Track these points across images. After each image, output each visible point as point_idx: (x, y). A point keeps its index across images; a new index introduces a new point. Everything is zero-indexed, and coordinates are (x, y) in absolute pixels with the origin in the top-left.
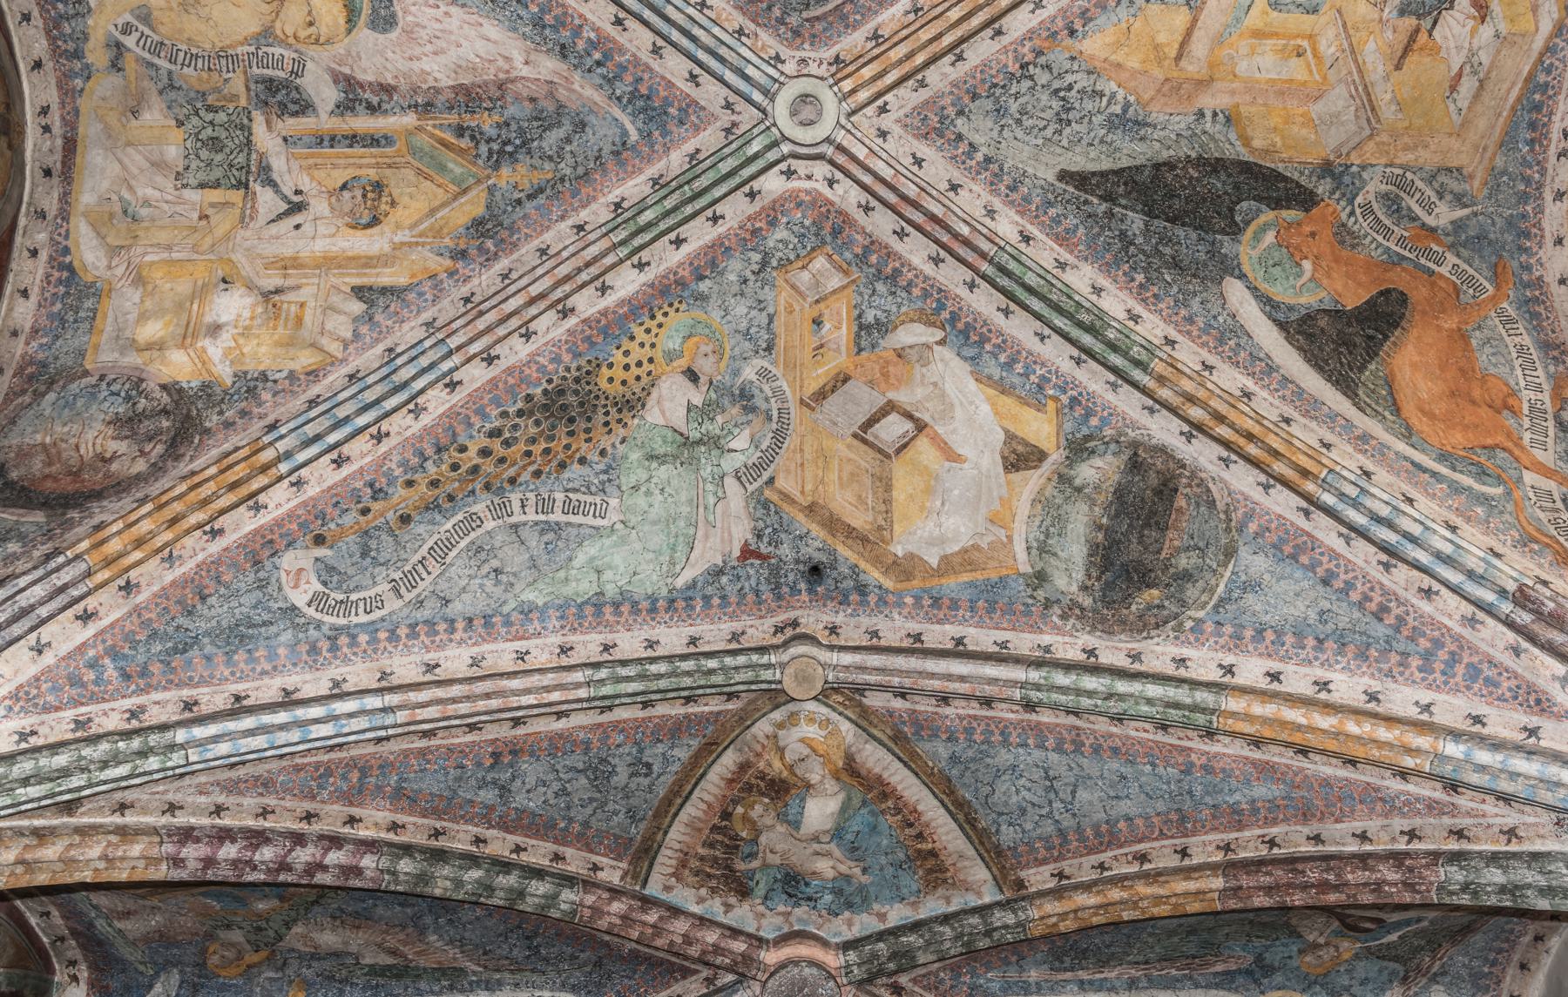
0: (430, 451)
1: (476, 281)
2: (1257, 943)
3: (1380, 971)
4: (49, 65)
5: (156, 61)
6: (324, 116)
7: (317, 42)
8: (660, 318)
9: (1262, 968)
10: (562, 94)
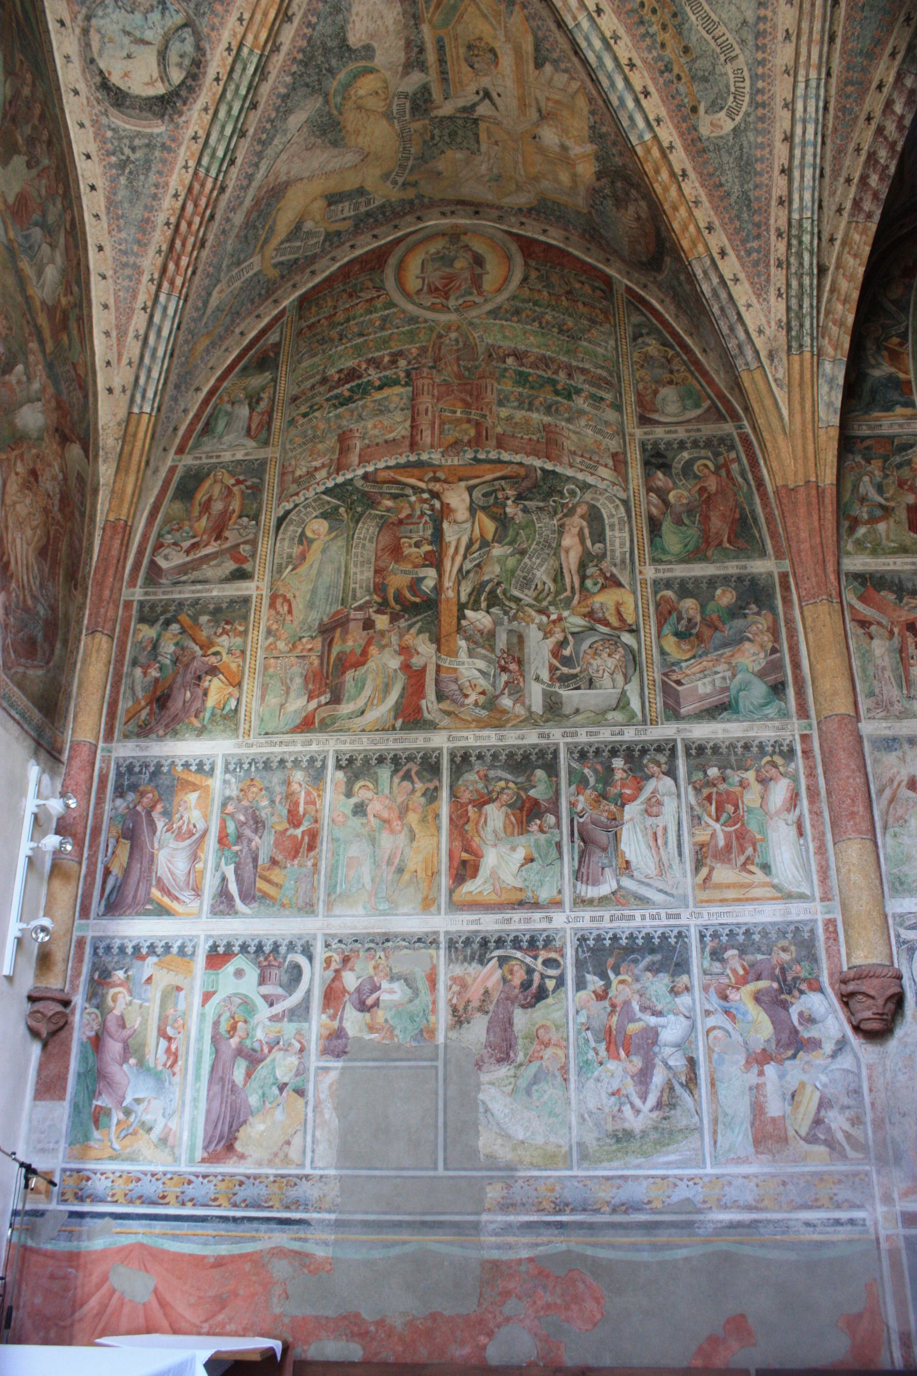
0: (642, 30)
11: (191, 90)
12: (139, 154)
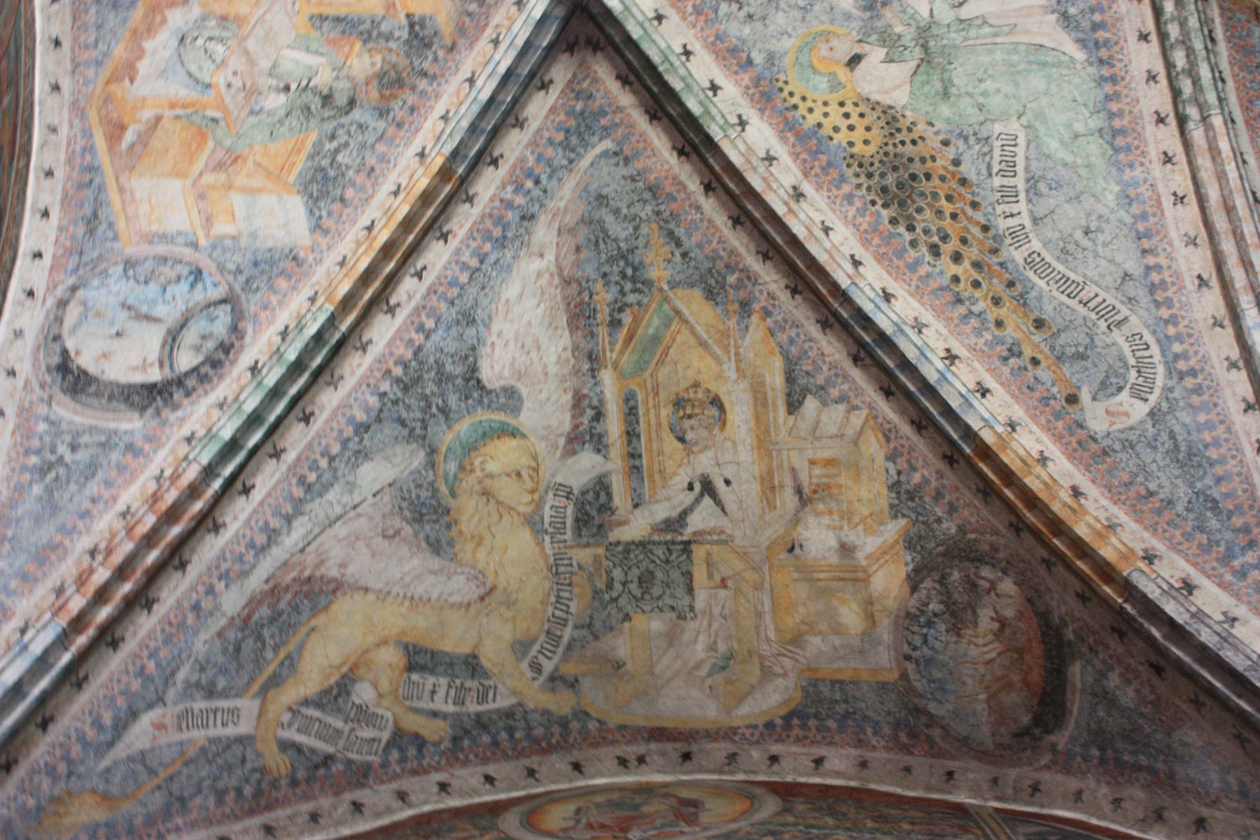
1: (773, 287)
4: (576, 755)
5: (565, 640)
6: (609, 466)
7: (536, 470)
8: (796, 100)
10: (570, 220)
11: (204, 379)
12: (82, 455)
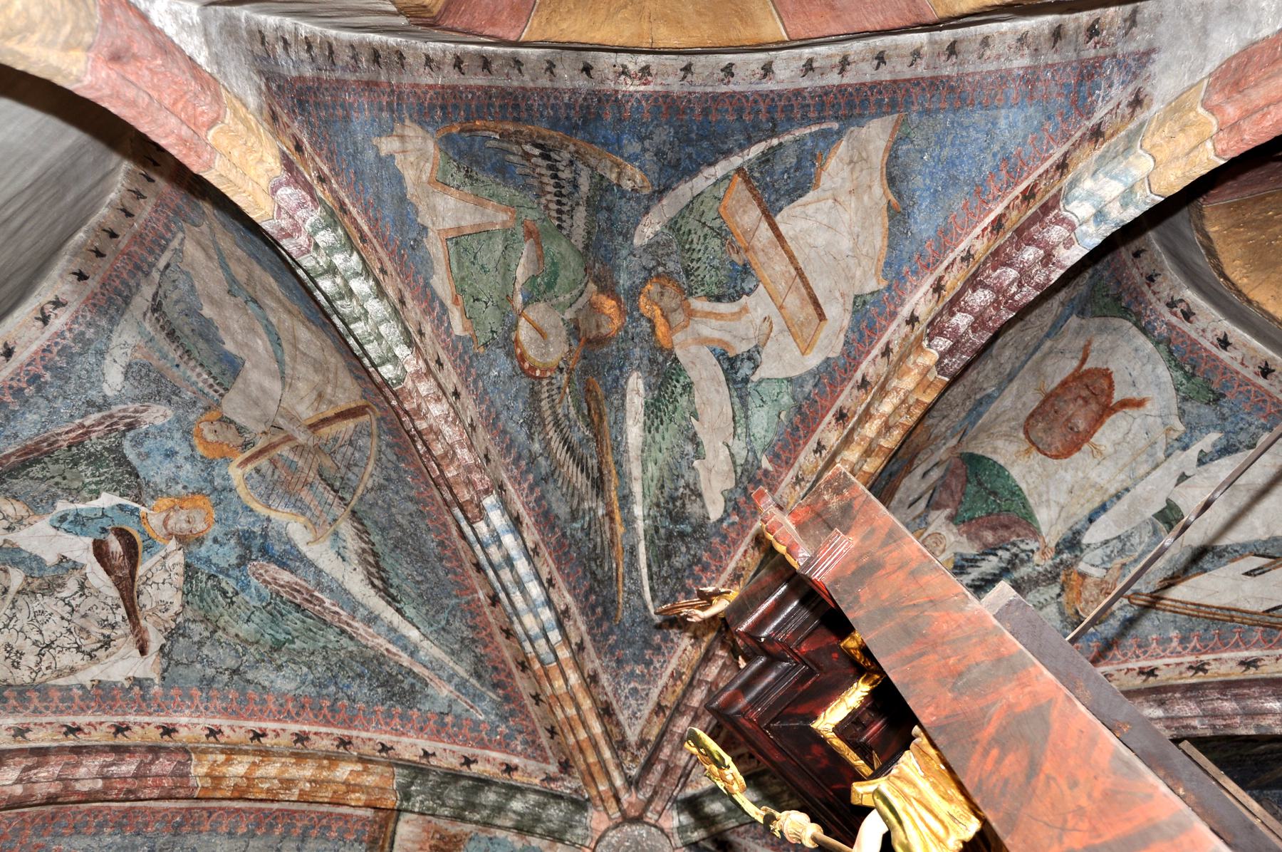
2: (229, 585)
3: (148, 455)
9: (248, 548)
